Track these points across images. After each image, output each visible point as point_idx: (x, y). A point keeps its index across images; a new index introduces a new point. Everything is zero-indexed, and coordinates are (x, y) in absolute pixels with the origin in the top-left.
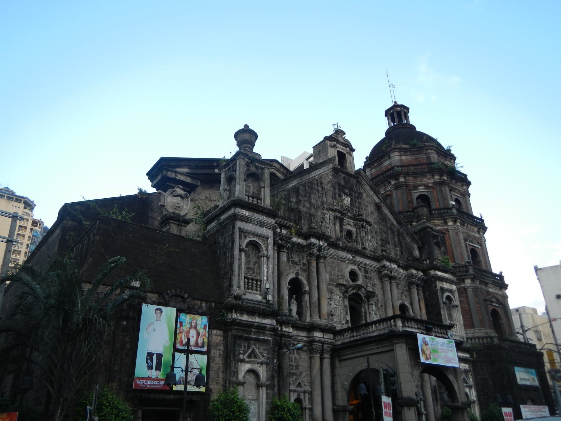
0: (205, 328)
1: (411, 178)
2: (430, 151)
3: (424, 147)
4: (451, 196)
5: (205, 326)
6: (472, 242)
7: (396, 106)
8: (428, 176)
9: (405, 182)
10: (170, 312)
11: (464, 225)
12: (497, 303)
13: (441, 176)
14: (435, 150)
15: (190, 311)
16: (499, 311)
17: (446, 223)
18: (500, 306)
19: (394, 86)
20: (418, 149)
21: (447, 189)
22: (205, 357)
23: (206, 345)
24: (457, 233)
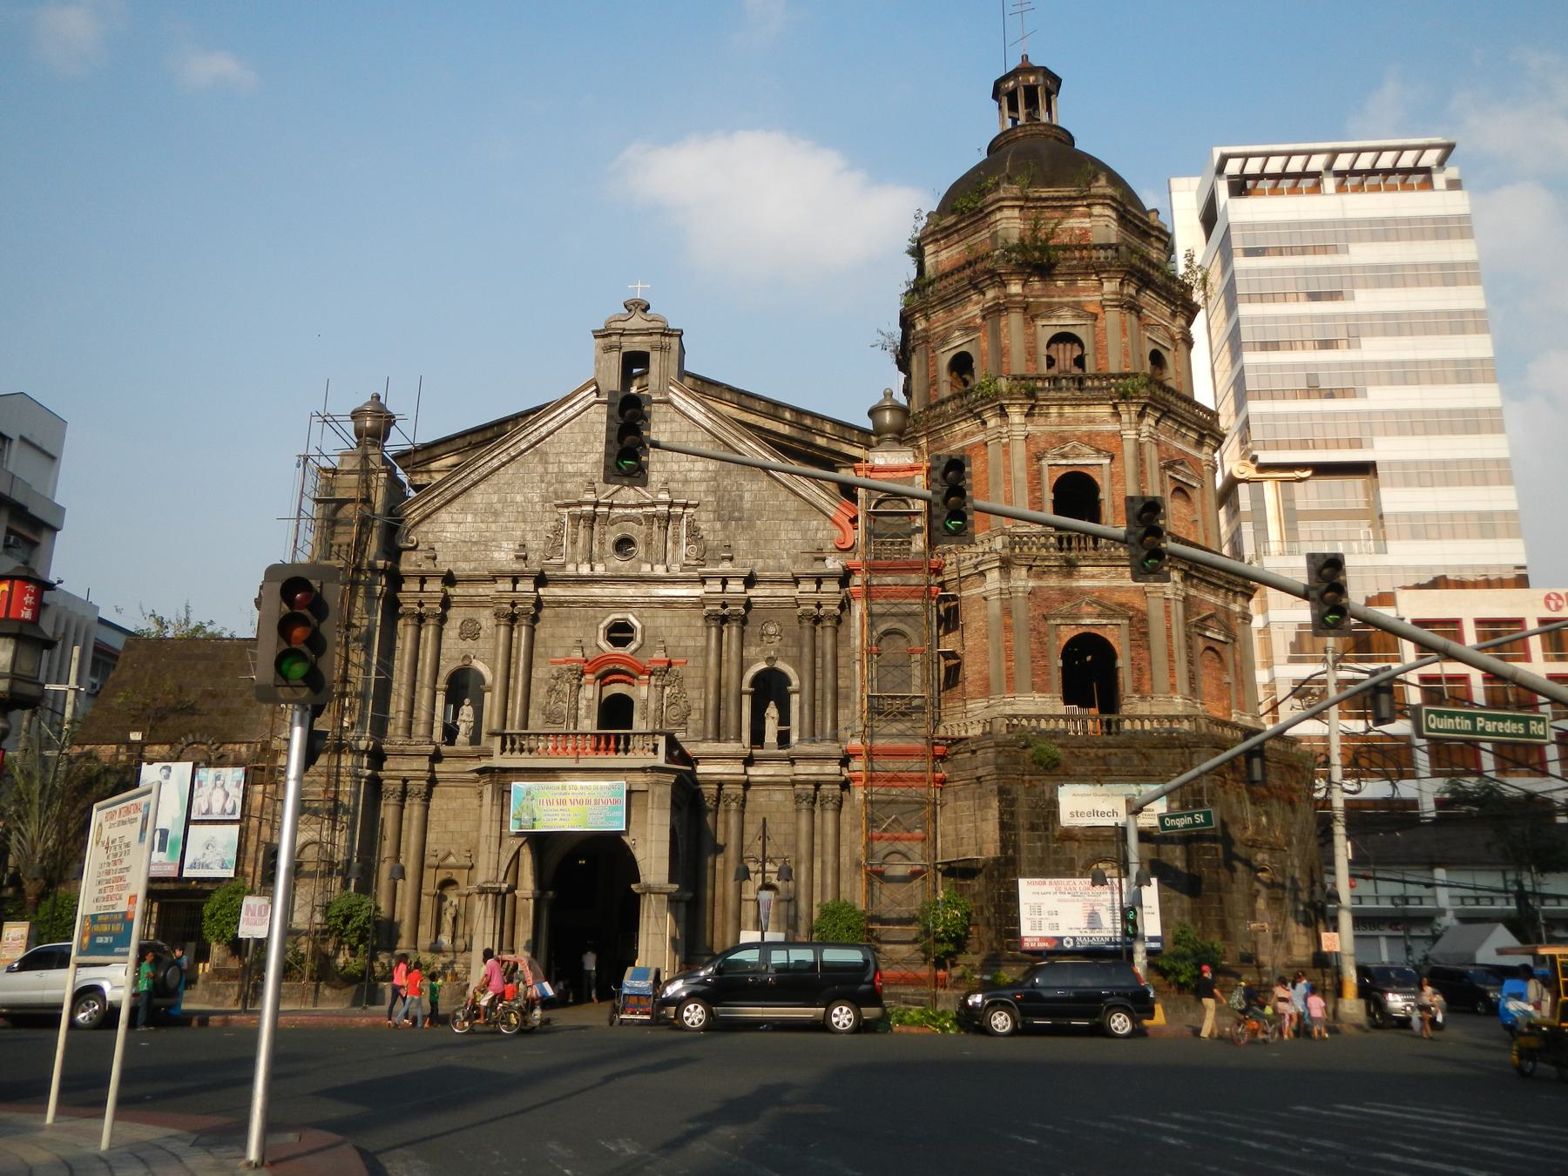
0: (238, 786)
1: (941, 314)
2: (998, 216)
3: (981, 210)
4: (1035, 334)
5: (239, 783)
6: (1064, 456)
7: (1026, 69)
8: (975, 298)
9: (924, 330)
10: (183, 769)
11: (1047, 415)
12: (1099, 616)
13: (1004, 285)
14: (1013, 207)
15: (221, 762)
16: (1117, 635)
17: (984, 423)
18: (1114, 622)
19: (1026, 7)
20: (972, 220)
21: (1014, 320)
22: (235, 828)
23: (239, 810)
24: (1007, 445)
